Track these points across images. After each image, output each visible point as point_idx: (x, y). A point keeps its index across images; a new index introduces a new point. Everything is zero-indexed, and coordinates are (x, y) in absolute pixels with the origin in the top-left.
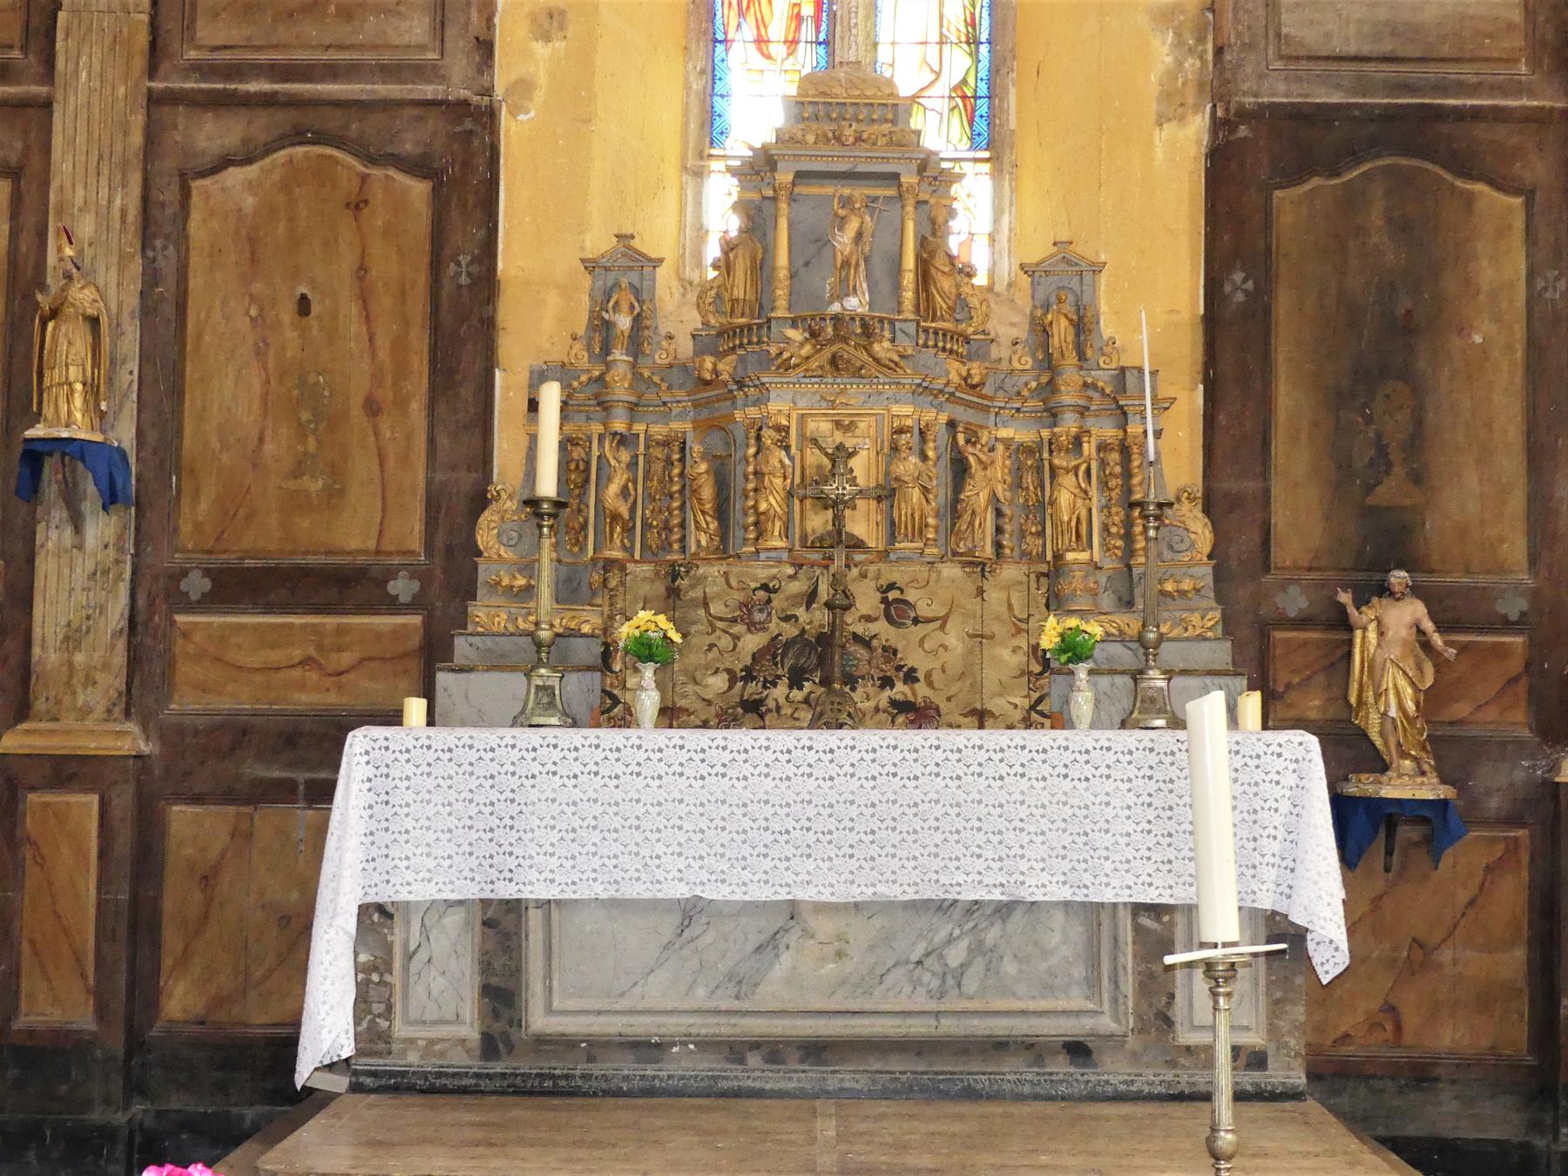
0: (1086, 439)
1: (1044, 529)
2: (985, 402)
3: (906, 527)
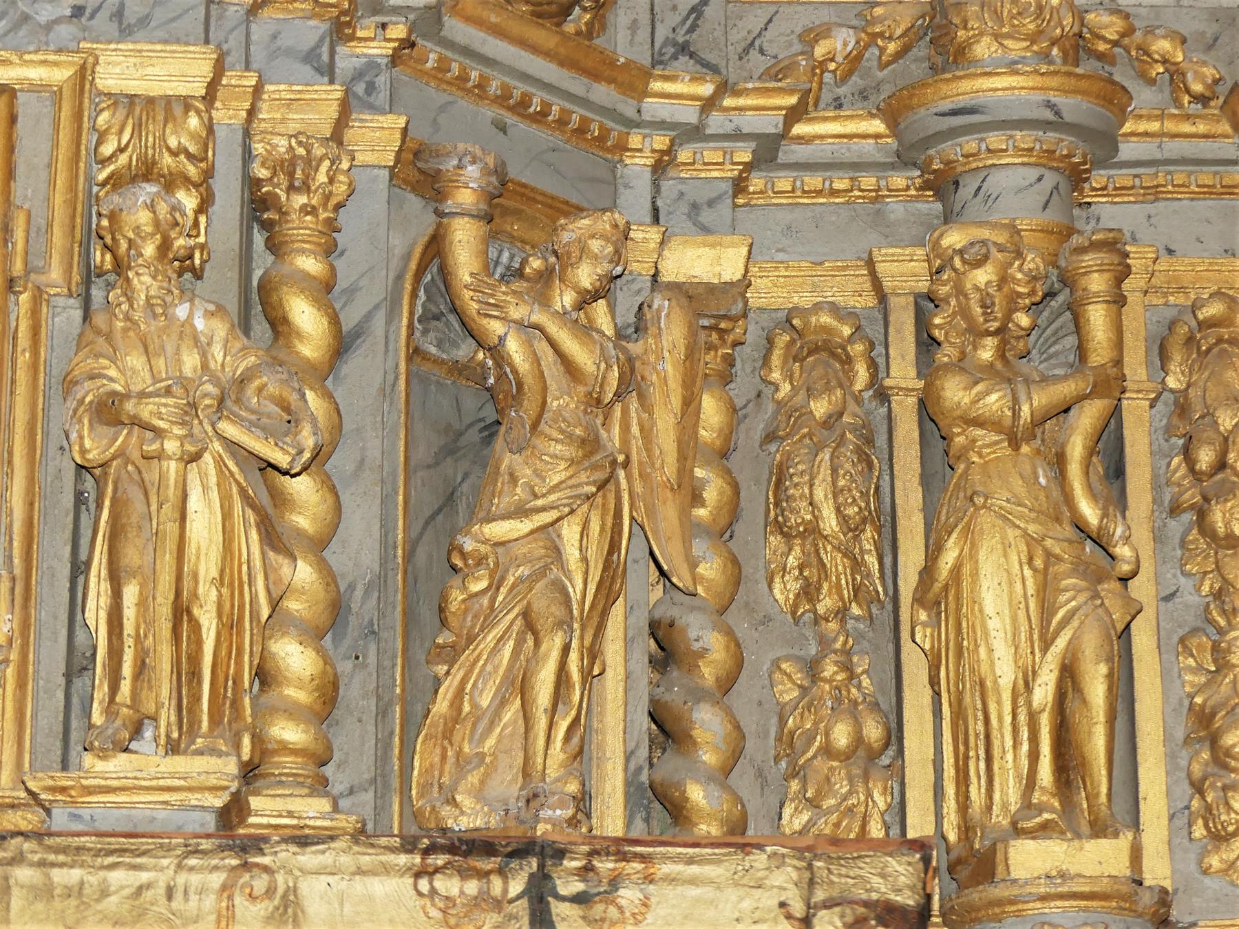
0: (1097, 283)
1: (895, 735)
2: (602, 93)
3: (141, 668)
